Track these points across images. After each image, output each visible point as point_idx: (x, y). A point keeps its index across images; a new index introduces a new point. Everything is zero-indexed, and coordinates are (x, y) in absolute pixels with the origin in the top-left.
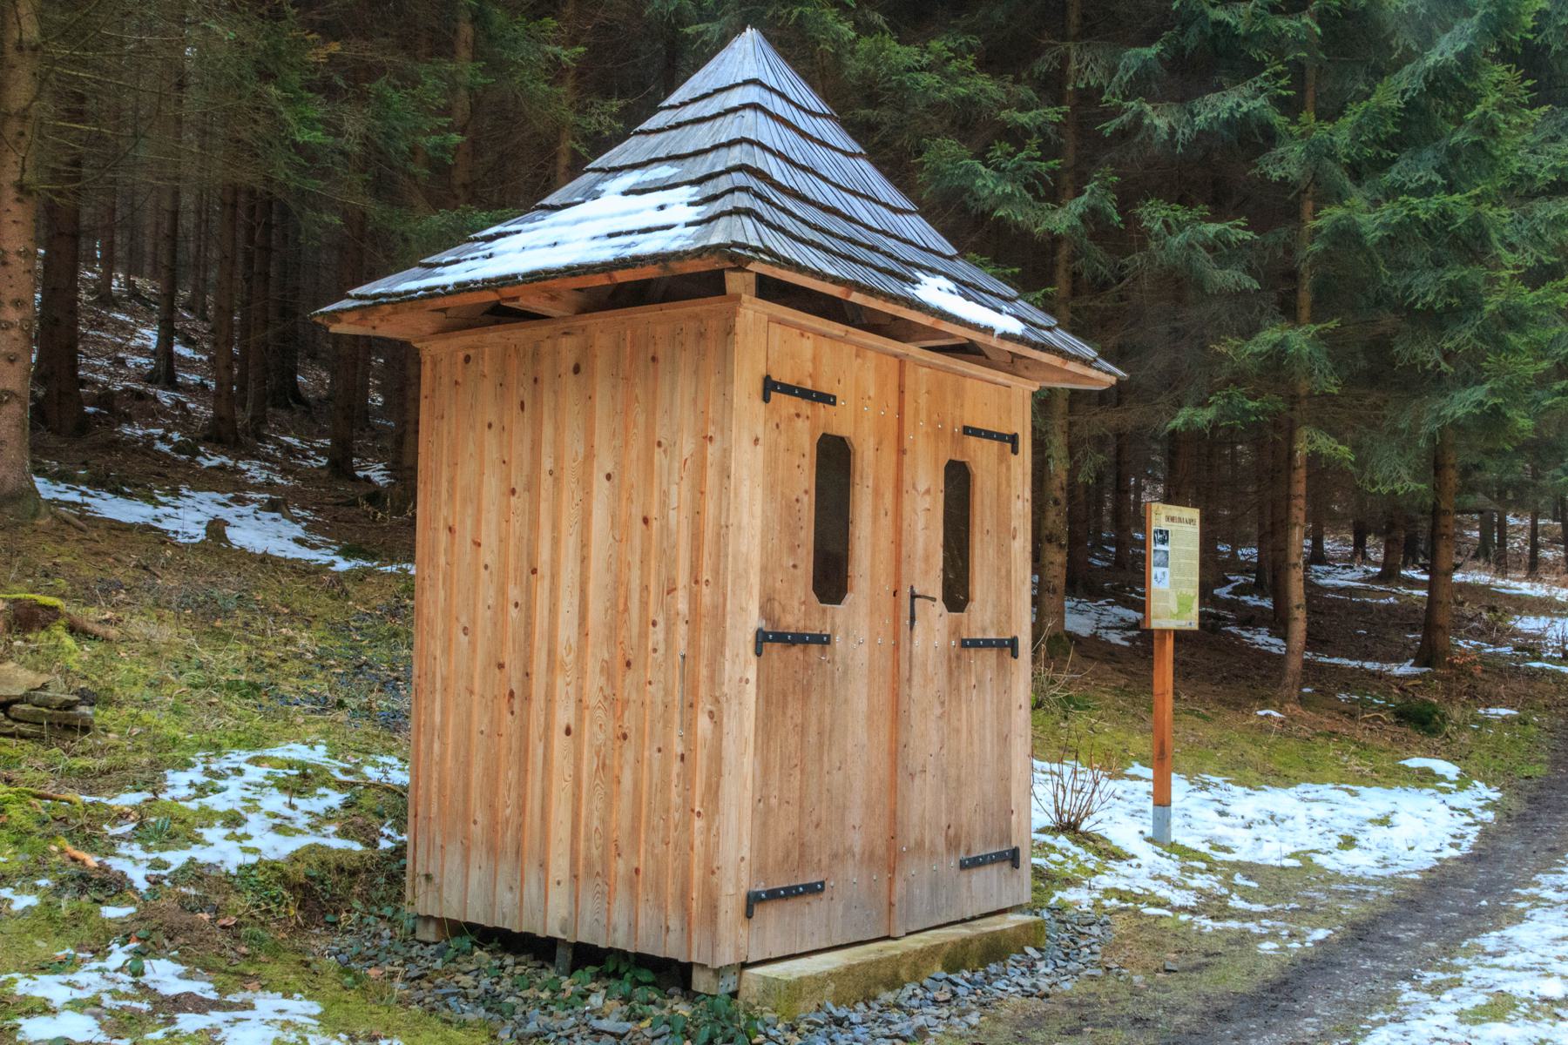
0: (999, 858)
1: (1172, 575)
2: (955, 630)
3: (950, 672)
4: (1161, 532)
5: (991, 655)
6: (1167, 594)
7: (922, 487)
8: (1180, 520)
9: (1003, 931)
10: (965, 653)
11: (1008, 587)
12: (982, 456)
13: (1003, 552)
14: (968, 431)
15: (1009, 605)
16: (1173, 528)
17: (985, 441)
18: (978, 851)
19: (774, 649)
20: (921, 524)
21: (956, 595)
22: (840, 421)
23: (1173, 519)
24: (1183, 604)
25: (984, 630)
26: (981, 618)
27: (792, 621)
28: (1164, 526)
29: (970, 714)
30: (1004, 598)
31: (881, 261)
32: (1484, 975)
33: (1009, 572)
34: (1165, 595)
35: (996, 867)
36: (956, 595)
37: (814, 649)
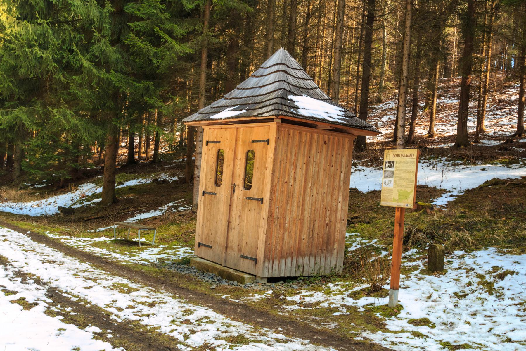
0: (251, 259)
1: (395, 181)
2: (245, 195)
3: (243, 206)
4: (389, 162)
5: (255, 203)
6: (392, 190)
7: (239, 158)
8: (403, 156)
9: (34, 201)
10: (247, 201)
11: (263, 183)
12: (258, 148)
13: (263, 174)
14: (254, 141)
15: (263, 189)
16: (398, 160)
17: (259, 143)
18: (246, 254)
19: (207, 195)
20: (238, 167)
21: (248, 187)
22: (221, 146)
23: (397, 156)
24: (403, 196)
25: (254, 195)
26: (253, 192)
27: (209, 190)
28: (392, 159)
29: (247, 217)
30: (261, 187)
31: (267, 103)
32: (46, 252)
33: (264, 180)
34: (391, 191)
35: (249, 260)
36: (248, 187)
37: (213, 196)
